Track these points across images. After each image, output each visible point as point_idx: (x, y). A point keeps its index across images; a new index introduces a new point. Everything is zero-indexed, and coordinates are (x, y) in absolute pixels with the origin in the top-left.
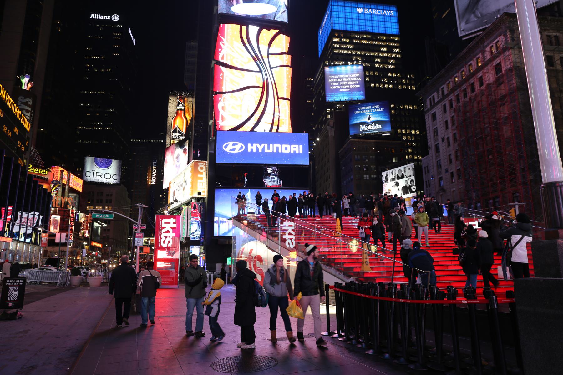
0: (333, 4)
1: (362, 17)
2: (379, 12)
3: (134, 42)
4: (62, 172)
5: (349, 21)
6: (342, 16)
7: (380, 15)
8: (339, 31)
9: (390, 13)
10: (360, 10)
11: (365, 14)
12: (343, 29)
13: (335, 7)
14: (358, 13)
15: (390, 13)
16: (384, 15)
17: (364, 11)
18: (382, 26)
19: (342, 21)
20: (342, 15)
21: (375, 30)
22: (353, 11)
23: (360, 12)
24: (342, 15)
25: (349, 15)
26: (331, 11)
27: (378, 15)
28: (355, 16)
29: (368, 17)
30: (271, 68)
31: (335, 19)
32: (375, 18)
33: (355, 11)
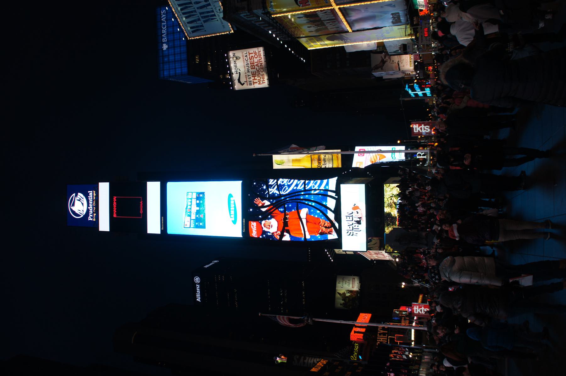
0: (162, 76)
1: (171, 44)
3: (216, 261)
4: (355, 332)
5: (178, 57)
9: (164, 14)
10: (165, 47)
13: (165, 73)
15: (164, 14)
17: (165, 43)
23: (167, 47)
25: (172, 58)
28: (171, 51)
33: (167, 52)
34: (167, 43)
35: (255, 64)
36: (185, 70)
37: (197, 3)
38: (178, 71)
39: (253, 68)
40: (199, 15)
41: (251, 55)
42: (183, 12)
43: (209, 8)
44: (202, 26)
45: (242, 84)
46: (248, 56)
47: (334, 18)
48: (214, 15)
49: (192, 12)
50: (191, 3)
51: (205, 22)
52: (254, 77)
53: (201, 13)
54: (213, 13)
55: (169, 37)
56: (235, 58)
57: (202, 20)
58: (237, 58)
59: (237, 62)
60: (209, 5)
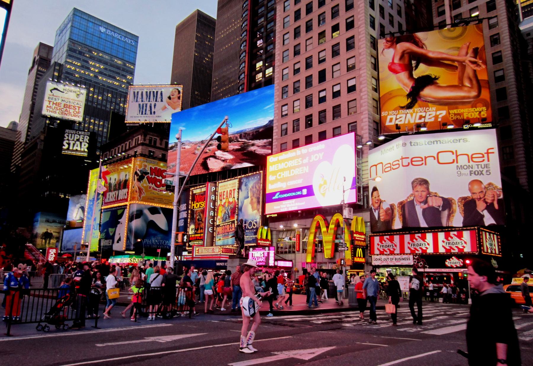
35: (68, 109)
37: (155, 105)
39: (64, 106)
40: (146, 103)
41: (77, 108)
42: (152, 93)
43: (148, 112)
44: (137, 101)
45: (51, 91)
46: (77, 105)
47: (119, 199)
48: (142, 114)
49: (149, 99)
50: (156, 101)
51: (140, 105)
52: (56, 104)
53: (146, 104)
54: (144, 113)
56: (78, 93)
57: (141, 103)
58: (78, 95)
59: (75, 94)
60: (151, 113)
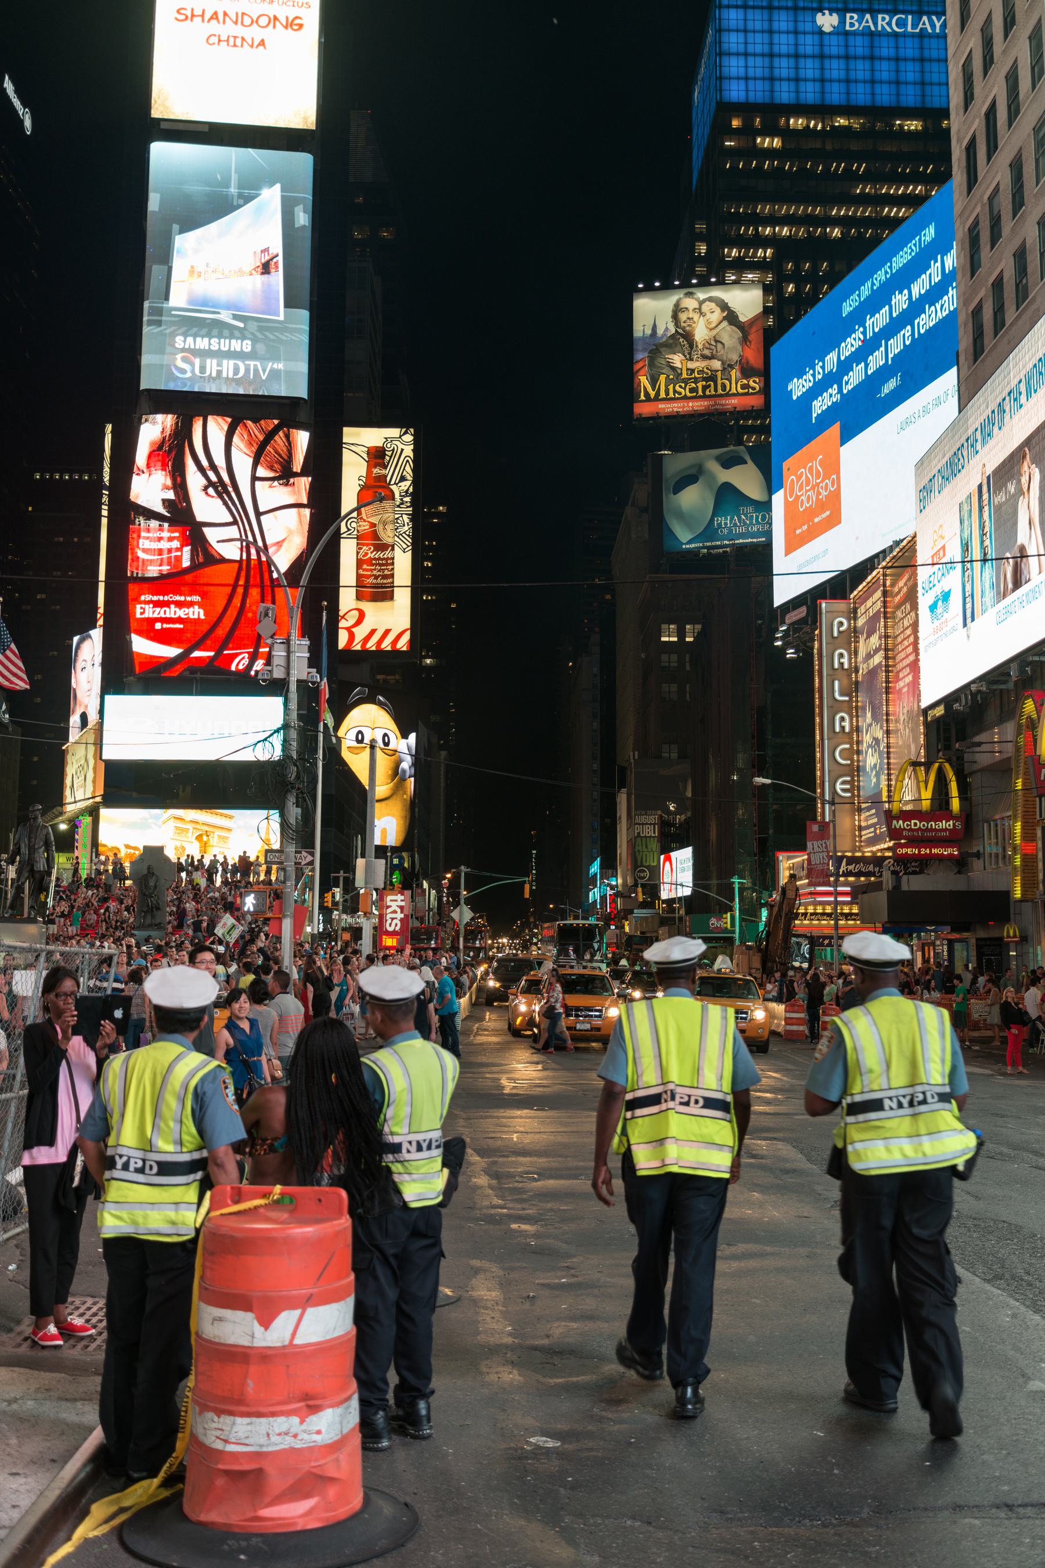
1: (834, 47)
2: (901, 23)
5: (784, 67)
6: (759, 49)
7: (905, 35)
8: (745, 109)
10: (827, 21)
11: (847, 33)
12: (760, 100)
14: (821, 33)
16: (922, 35)
17: (842, 21)
18: (910, 77)
19: (757, 66)
20: (758, 43)
21: (885, 96)
22: (801, 27)
23: (827, 29)
24: (758, 43)
25: (784, 43)
26: (720, 31)
27: (896, 35)
28: (809, 45)
29: (859, 46)
30: (258, 514)
31: (733, 61)
32: (886, 49)
33: (808, 27)
34: (839, 31)
36: (735, 92)
38: (734, 66)
55: (859, 41)
